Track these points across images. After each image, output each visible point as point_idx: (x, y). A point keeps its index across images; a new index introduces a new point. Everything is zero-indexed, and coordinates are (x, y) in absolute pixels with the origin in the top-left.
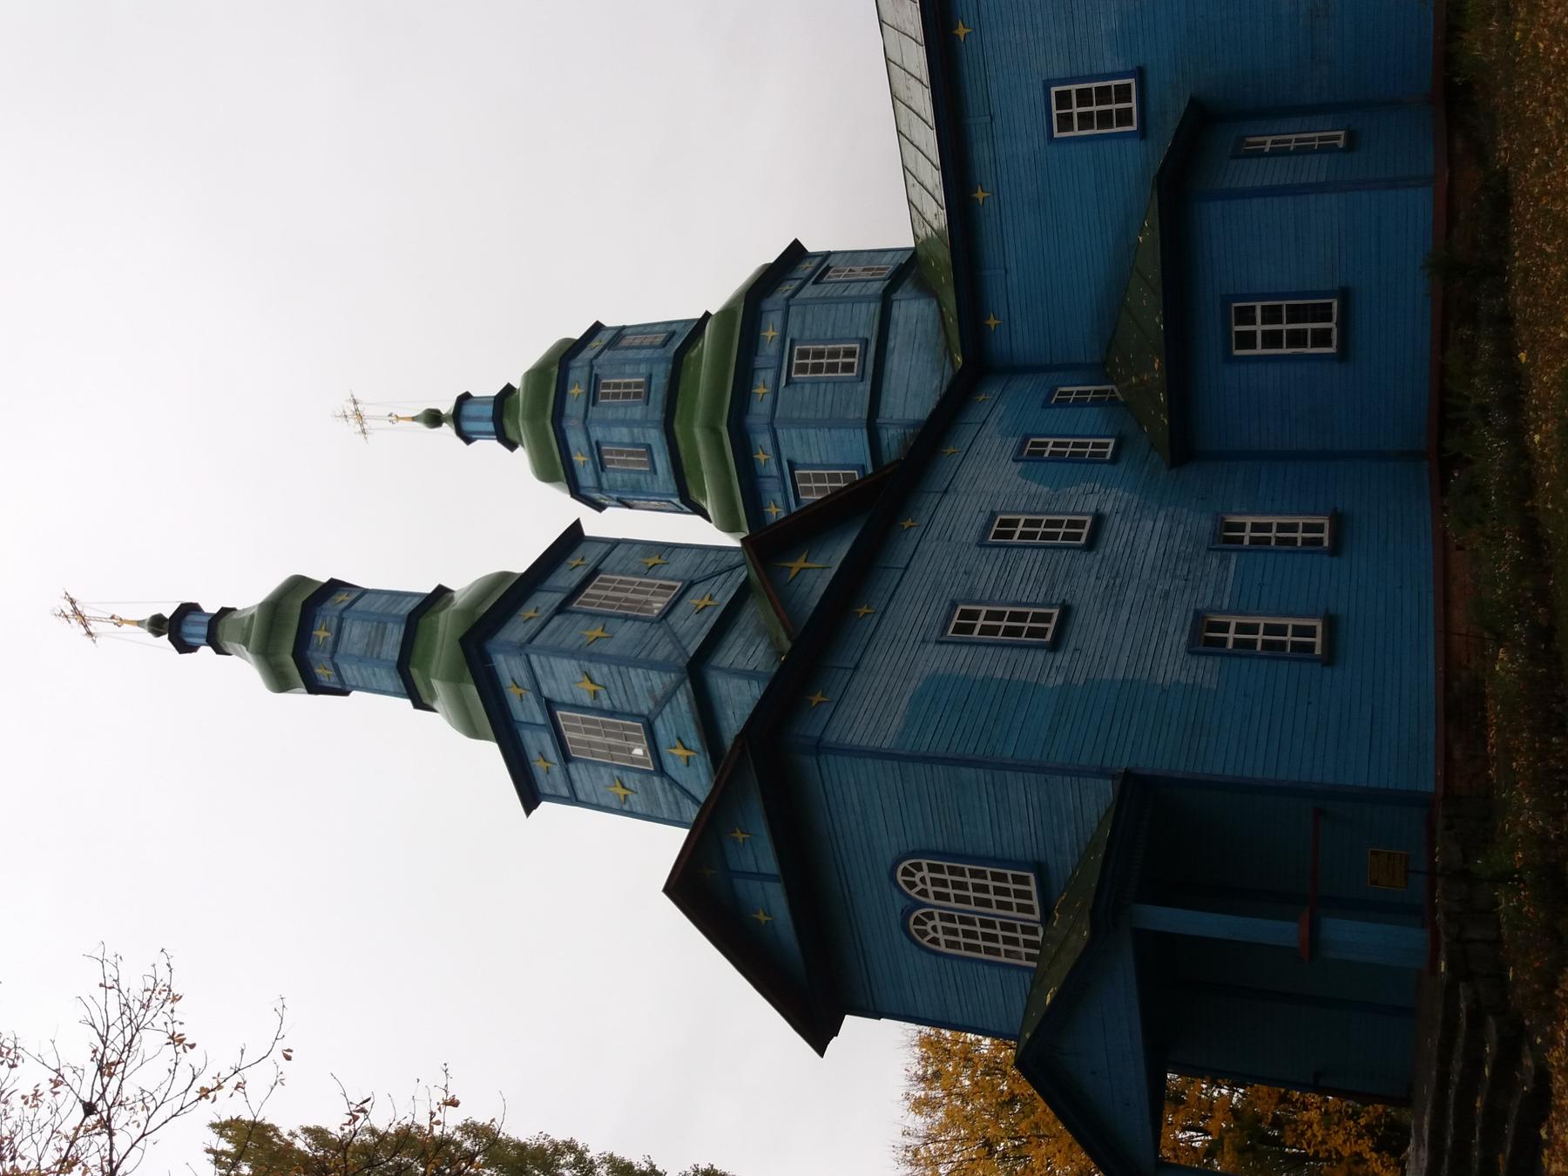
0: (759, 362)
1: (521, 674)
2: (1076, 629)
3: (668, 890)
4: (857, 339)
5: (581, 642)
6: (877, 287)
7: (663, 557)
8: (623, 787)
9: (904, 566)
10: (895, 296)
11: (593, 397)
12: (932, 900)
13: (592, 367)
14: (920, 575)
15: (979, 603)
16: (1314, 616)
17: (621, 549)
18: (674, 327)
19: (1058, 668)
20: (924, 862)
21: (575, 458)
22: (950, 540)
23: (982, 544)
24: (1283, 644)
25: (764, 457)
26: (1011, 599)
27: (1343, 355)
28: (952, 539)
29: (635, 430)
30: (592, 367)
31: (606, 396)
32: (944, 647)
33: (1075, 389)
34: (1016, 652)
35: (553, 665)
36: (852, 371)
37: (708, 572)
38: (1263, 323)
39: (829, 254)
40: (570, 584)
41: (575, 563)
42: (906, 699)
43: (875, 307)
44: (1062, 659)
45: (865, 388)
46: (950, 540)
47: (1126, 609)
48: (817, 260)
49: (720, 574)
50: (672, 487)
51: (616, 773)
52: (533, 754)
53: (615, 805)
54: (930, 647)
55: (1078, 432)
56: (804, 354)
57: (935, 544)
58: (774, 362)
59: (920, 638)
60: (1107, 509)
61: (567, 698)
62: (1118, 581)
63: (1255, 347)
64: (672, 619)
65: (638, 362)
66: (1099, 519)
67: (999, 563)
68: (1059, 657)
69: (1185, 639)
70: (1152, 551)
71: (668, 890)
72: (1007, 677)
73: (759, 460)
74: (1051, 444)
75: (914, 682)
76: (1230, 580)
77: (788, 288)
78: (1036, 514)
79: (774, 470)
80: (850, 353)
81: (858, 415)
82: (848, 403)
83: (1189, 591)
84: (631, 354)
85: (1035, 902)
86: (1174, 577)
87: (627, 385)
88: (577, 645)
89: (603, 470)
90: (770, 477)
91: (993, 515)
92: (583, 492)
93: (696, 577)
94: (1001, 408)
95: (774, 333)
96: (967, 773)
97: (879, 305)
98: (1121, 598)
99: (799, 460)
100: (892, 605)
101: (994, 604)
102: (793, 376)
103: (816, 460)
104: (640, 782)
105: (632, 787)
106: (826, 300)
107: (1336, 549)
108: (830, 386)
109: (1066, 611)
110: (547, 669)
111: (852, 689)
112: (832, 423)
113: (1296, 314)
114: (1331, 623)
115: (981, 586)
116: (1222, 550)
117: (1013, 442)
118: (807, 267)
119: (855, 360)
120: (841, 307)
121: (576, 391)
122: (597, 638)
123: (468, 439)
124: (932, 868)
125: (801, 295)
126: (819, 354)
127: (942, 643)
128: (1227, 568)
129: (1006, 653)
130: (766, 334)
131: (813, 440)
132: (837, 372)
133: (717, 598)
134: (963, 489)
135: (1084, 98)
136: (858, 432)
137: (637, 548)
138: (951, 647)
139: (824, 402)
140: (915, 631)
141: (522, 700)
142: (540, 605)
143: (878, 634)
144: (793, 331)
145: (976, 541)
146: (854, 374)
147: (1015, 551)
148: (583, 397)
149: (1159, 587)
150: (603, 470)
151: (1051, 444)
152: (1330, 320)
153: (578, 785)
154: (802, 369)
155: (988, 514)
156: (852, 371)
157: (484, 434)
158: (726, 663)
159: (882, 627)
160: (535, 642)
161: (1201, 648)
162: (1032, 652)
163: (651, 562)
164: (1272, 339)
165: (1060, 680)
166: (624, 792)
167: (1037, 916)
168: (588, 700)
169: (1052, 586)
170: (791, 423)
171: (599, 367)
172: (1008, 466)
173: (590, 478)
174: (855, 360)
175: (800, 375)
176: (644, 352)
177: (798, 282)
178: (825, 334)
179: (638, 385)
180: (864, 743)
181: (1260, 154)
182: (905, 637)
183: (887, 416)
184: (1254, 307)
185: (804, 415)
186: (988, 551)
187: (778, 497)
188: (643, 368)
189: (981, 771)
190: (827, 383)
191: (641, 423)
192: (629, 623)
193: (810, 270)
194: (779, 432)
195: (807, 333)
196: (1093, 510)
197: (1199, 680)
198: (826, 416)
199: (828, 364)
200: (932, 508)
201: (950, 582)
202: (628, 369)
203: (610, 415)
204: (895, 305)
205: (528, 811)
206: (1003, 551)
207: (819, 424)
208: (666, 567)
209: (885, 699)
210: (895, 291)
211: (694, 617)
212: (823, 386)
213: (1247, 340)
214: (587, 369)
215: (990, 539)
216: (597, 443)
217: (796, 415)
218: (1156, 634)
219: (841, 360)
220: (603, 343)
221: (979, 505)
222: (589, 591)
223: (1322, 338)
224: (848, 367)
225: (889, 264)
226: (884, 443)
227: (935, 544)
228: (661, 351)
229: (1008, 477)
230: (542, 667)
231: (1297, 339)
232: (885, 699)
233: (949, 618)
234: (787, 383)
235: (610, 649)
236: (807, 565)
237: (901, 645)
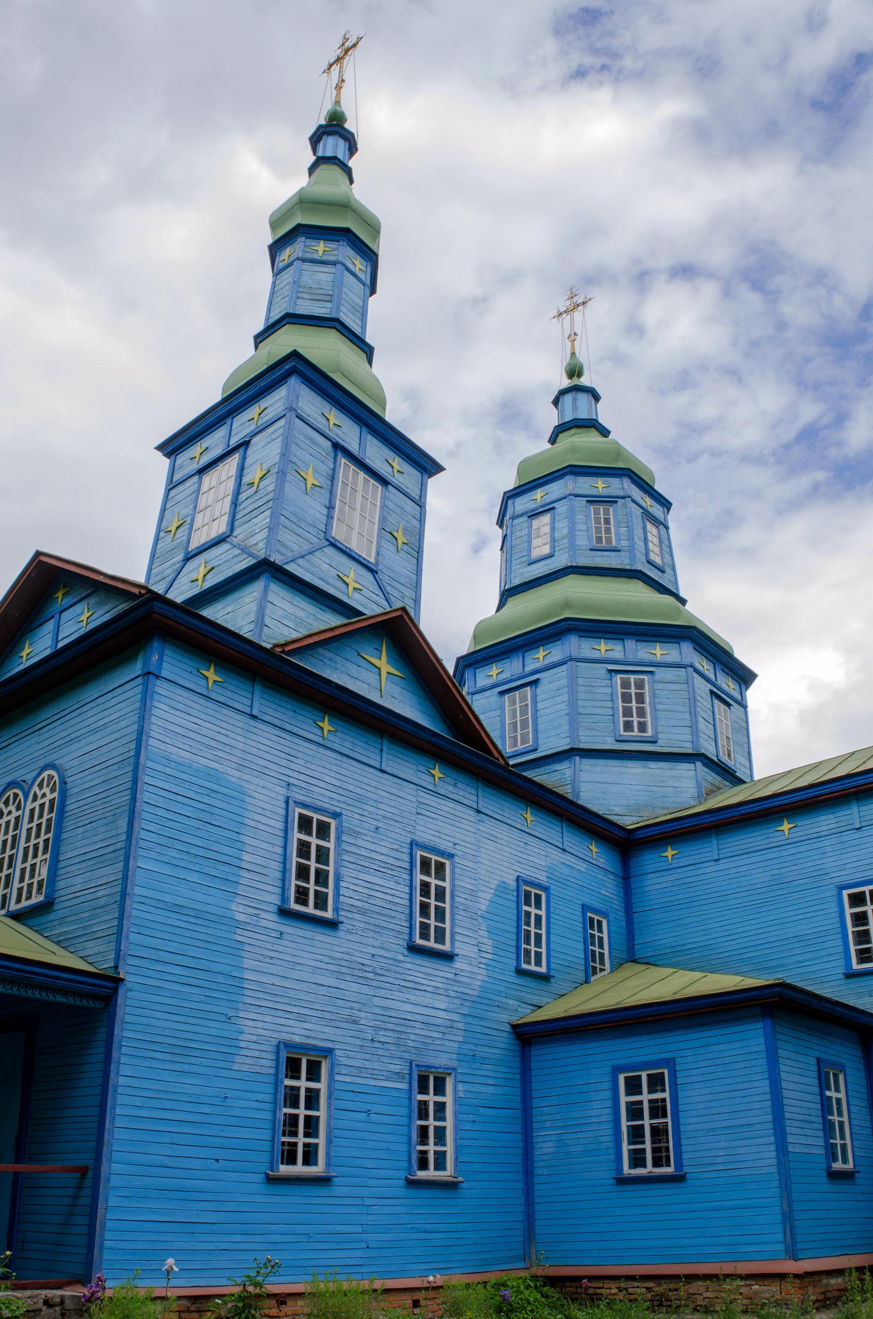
0: (630, 644)
1: (268, 416)
2: (308, 934)
3: (38, 554)
5: (299, 463)
6: (710, 750)
7: (405, 547)
8: (178, 528)
9: (384, 768)
10: (699, 764)
11: (594, 500)
12: (29, 806)
13: (623, 498)
14: (373, 783)
15: (338, 839)
16: (328, 1164)
17: (413, 508)
18: (668, 571)
19: (257, 916)
20: (55, 794)
21: (539, 490)
22: (418, 814)
23: (413, 844)
24: (295, 1134)
25: (540, 656)
26: (344, 871)
27: (623, 1181)
28: (419, 816)
29: (566, 541)
30: (623, 498)
31: (597, 512)
32: (283, 805)
33: (605, 935)
34: (278, 875)
35: (276, 441)
36: (625, 731)
37: (388, 589)
38: (650, 1101)
39: (744, 707)
40: (369, 458)
41: (395, 464)
42: (215, 766)
43: (688, 748)
44: (270, 920)
45: (609, 744)
46: (418, 814)
47: (332, 982)
48: (739, 697)
49: (387, 600)
50: (517, 581)
51: (189, 519)
52: (206, 442)
53: (164, 524)
54: (283, 791)
55: (553, 938)
57: (414, 799)
58: (631, 657)
59: (292, 781)
60: (458, 964)
61: (248, 461)
62: (371, 976)
63: (628, 1094)
64: (330, 551)
65: (630, 538)
66: (448, 957)
67: (391, 861)
68: (275, 917)
69: (297, 1039)
70: (409, 1007)
71: (38, 554)
72: (244, 865)
73: (539, 652)
74: (538, 912)
75: (237, 774)
76: (373, 1082)
77: (706, 667)
78: (452, 897)
79: (529, 668)
80: (642, 727)
81: (582, 739)
82: (594, 729)
83: (359, 1042)
84: (638, 533)
85: (24, 904)
86: (377, 1029)
87: (608, 531)
88: (295, 460)
89: (529, 517)
90: (524, 666)
91: (451, 856)
92: (510, 502)
93: (380, 575)
94: (582, 866)
95: (658, 656)
96: (123, 825)
97: (690, 751)
98: (349, 978)
100: (335, 755)
101: (337, 855)
102: (619, 676)
103: (540, 706)
104: (182, 541)
105: (177, 536)
106: (693, 702)
107: (413, 1183)
108: (610, 712)
109: (332, 925)
110: (274, 436)
111: (225, 712)
112: (574, 715)
113: (658, 1133)
114: (324, 1181)
115: (360, 842)
116: (410, 1074)
117: (542, 877)
118: (729, 685)
119: (636, 732)
120: (687, 716)
121: (600, 486)
122: (306, 480)
123: (556, 402)
124: (52, 801)
125: (697, 679)
126: (640, 698)
127: (287, 802)
128: (388, 1079)
129: (277, 866)
130: (658, 648)
131: (559, 699)
132: (624, 716)
133: (357, 595)
134: (482, 829)
136: (568, 740)
137: (416, 523)
138: (283, 812)
139: (594, 707)
140: (302, 777)
141: (249, 421)
142: (344, 429)
143: (298, 741)
144: (660, 673)
145: (417, 839)
146: (622, 733)
147: (407, 877)
148: (593, 492)
149: (363, 1015)
150: (529, 517)
151: (538, 912)
152: (657, 1163)
153: (181, 488)
154: (625, 684)
155: (453, 851)
156: (625, 731)
157: (561, 414)
158: (271, 597)
159: (306, 744)
160: (297, 420)
161: (284, 1055)
162: (278, 891)
163: (401, 538)
164: (635, 1111)
165: (242, 918)
166: (173, 529)
167: (13, 907)
168: (246, 480)
169: (363, 912)
170: (573, 678)
171: (624, 504)
172: (510, 871)
173: (522, 507)
174: (636, 732)
175: (619, 683)
176: (642, 544)
177: (712, 677)
178: (660, 703)
179: (609, 540)
180: (154, 719)
181: (823, 1084)
182: (294, 766)
183: (582, 767)
184: (664, 1090)
185: (581, 689)
186: (407, 851)
187: (506, 675)
188: (624, 543)
189: (124, 837)
190: (613, 708)
191: (573, 548)
192: (325, 511)
193: (724, 687)
194: (564, 668)
195: (660, 686)
196: (457, 951)
197: (243, 1052)
198: (580, 710)
199: (631, 708)
200: (456, 798)
201: (366, 813)
202: (623, 530)
203: (580, 518)
204: (691, 766)
205: (160, 448)
206: (407, 866)
207: (573, 703)
208: (394, 550)
209: (213, 743)
210: (704, 765)
211: (334, 573)
212: (610, 704)
213: (633, 1086)
214: (622, 494)
215: (419, 853)
216: (553, 508)
217: (580, 681)
218: (303, 1011)
219: (635, 720)
220: (650, 509)
221: (461, 843)
223: (637, 1160)
224: (628, 726)
225: (736, 763)
226: (557, 767)
227: (414, 799)
228: (644, 559)
229: (497, 872)
230: (275, 431)
231: (636, 1134)
232: (213, 743)
233: (317, 810)
234: (611, 671)
235: (291, 490)
236: (384, 675)
237: (284, 763)
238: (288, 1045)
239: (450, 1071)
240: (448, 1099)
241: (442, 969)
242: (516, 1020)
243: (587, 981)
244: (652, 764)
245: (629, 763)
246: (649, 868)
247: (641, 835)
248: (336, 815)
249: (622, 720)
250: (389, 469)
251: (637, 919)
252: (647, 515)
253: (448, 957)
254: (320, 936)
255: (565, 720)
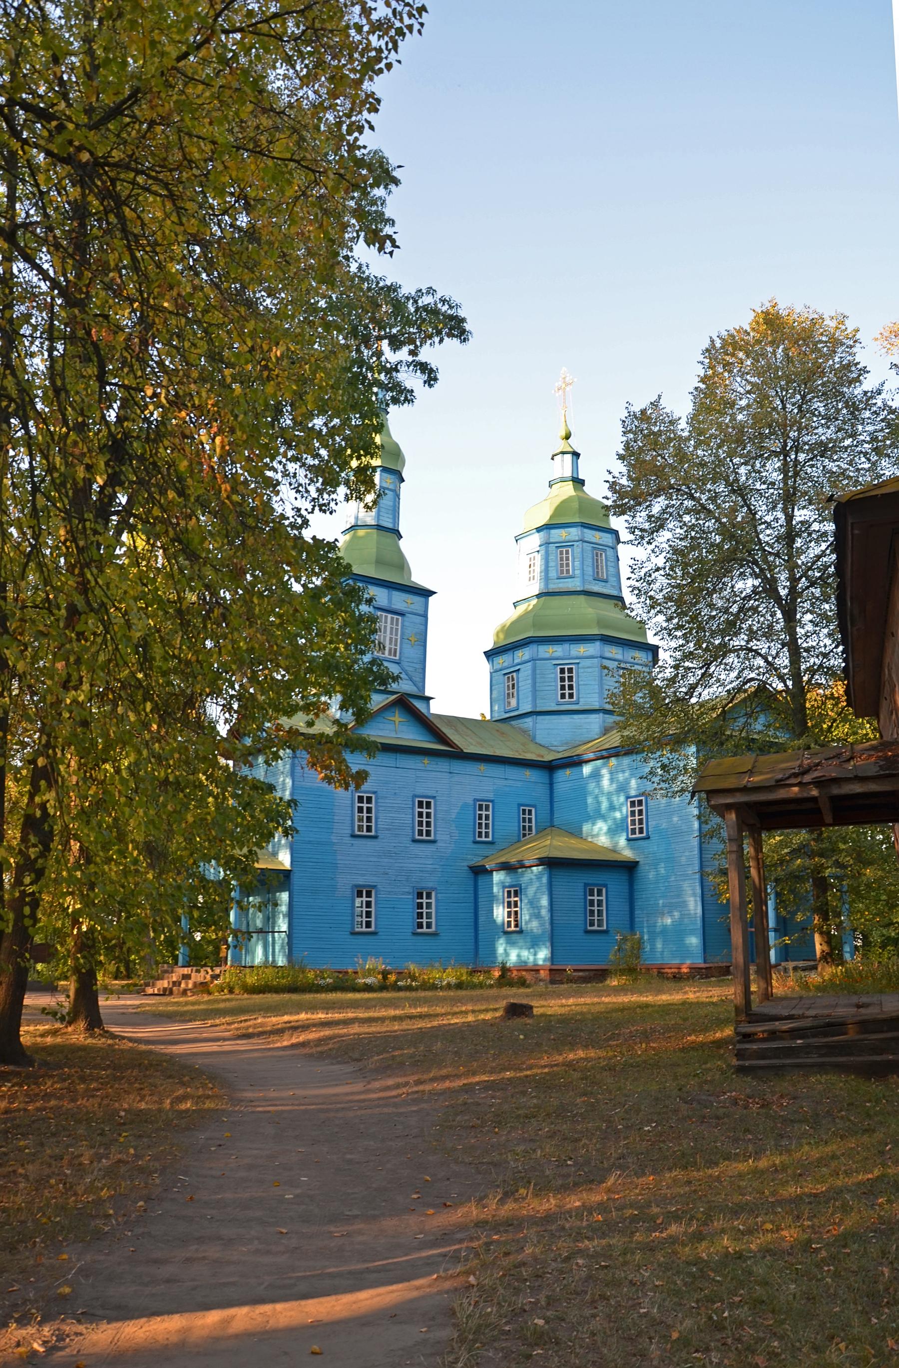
0: (566, 646)
4: (578, 698)
23: (416, 796)
44: (348, 840)
56: (570, 670)
60: (439, 844)
66: (434, 842)
80: (571, 696)
91: (434, 797)
99: (521, 674)
109: (375, 837)
117: (491, 796)
119: (567, 699)
126: (570, 679)
135: (640, 812)
137: (423, 627)
144: (585, 663)
163: (413, 639)
169: (389, 829)
170: (534, 670)
177: (620, 657)
187: (506, 664)
202: (577, 564)
222: (389, 616)
224: (563, 696)
238: (356, 886)
239: (435, 889)
240: (433, 901)
241: (431, 848)
242: (471, 863)
243: (519, 841)
244: (576, 716)
245: (563, 717)
246: (560, 780)
247: (554, 763)
248: (375, 793)
249: (560, 692)
250: (405, 605)
251: (556, 805)
252: (598, 549)
253: (434, 842)
254: (370, 843)
255: (530, 694)
